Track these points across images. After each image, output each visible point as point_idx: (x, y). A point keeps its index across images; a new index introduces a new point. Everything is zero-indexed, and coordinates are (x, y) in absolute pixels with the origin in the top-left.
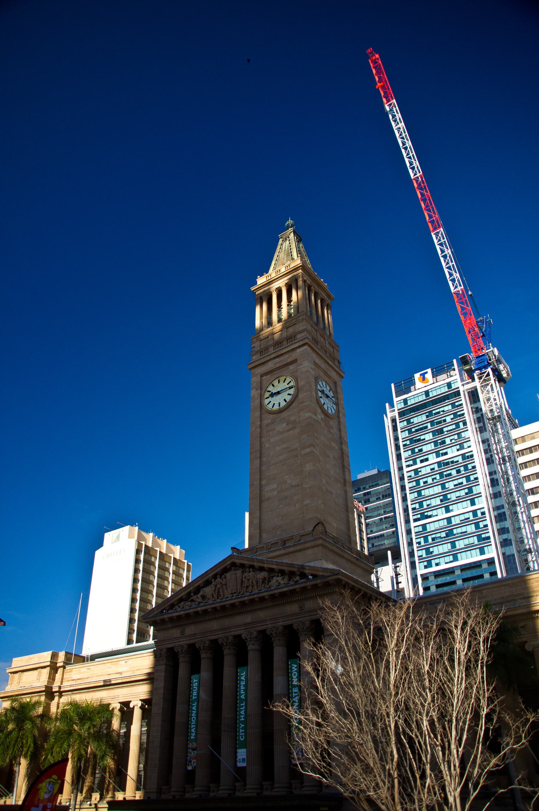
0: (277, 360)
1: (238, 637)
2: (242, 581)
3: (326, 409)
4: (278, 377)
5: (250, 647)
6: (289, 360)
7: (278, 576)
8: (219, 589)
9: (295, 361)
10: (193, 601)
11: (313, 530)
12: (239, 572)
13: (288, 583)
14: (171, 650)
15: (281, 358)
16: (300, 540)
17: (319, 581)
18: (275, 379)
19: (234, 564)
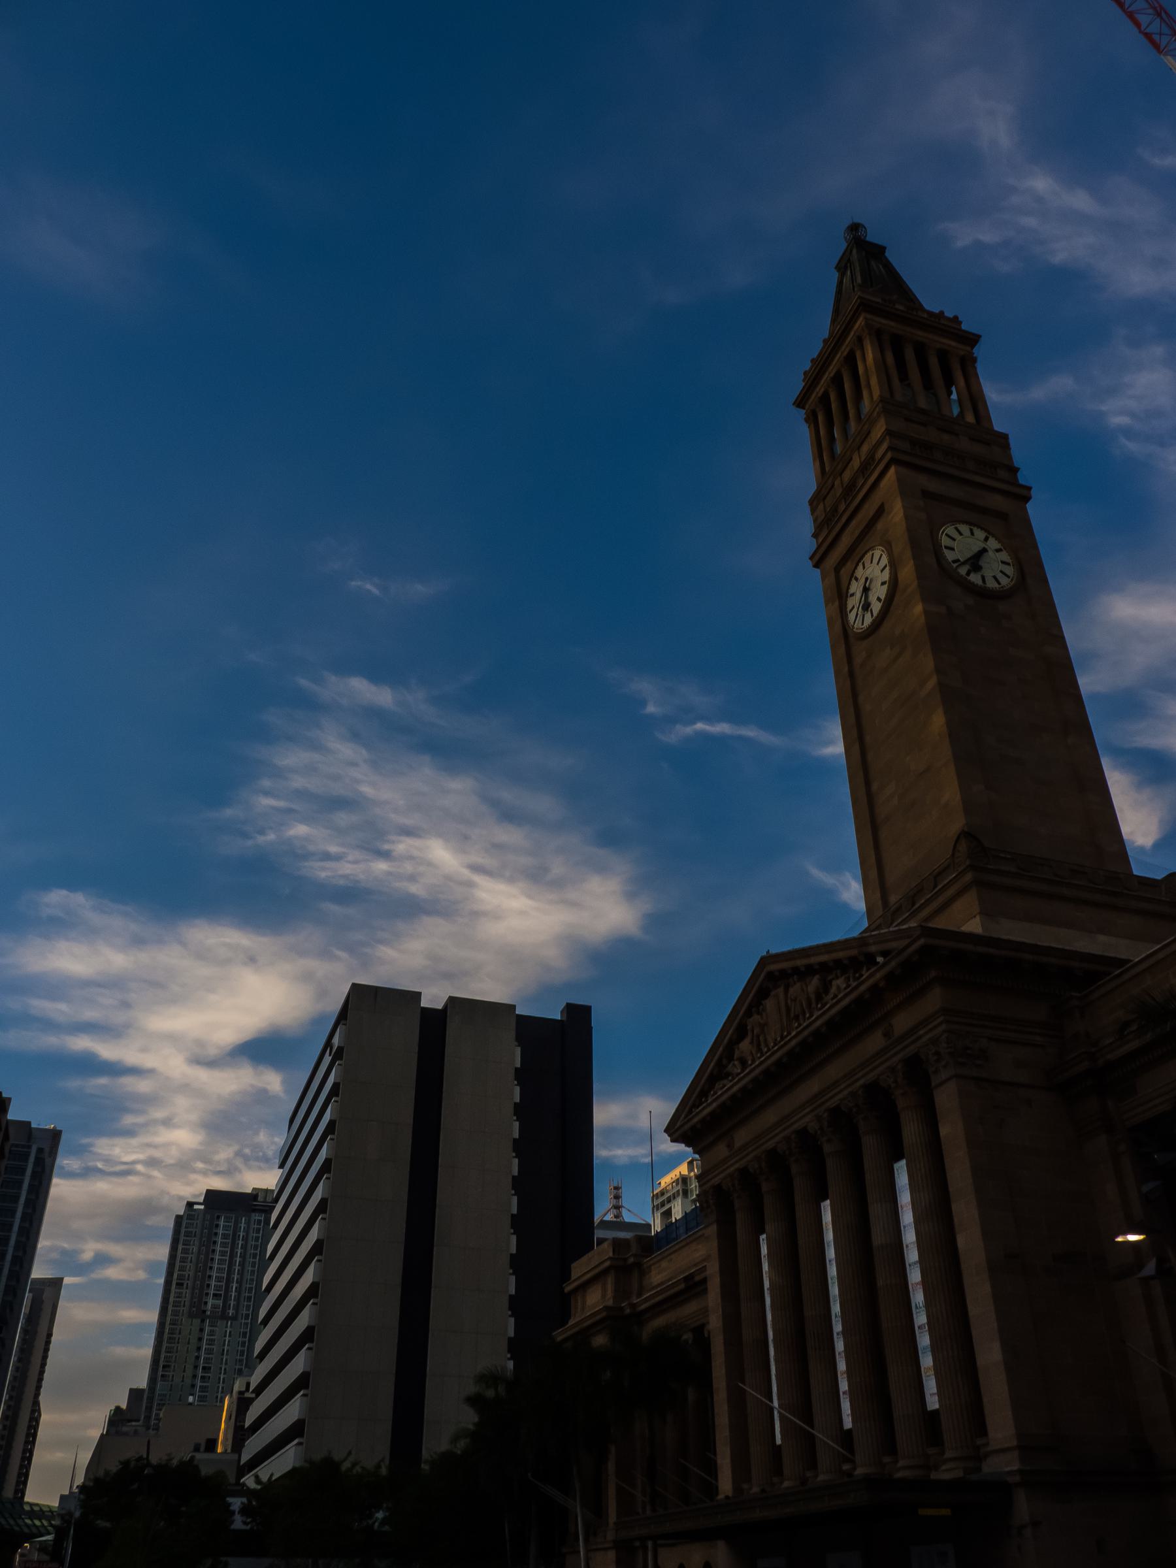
0: (854, 522)
1: (803, 1133)
2: (788, 1010)
3: (980, 582)
4: (862, 558)
5: (827, 1148)
6: (871, 513)
7: (837, 978)
8: (758, 1037)
9: (880, 511)
10: (728, 1074)
11: (953, 855)
12: (781, 991)
13: (848, 986)
14: (718, 1188)
15: (860, 516)
16: (935, 886)
17: (893, 964)
18: (857, 565)
19: (770, 975)
